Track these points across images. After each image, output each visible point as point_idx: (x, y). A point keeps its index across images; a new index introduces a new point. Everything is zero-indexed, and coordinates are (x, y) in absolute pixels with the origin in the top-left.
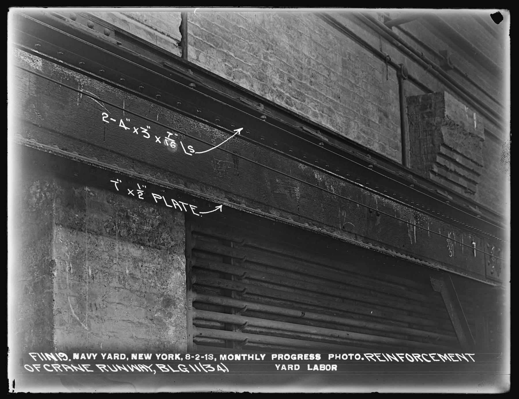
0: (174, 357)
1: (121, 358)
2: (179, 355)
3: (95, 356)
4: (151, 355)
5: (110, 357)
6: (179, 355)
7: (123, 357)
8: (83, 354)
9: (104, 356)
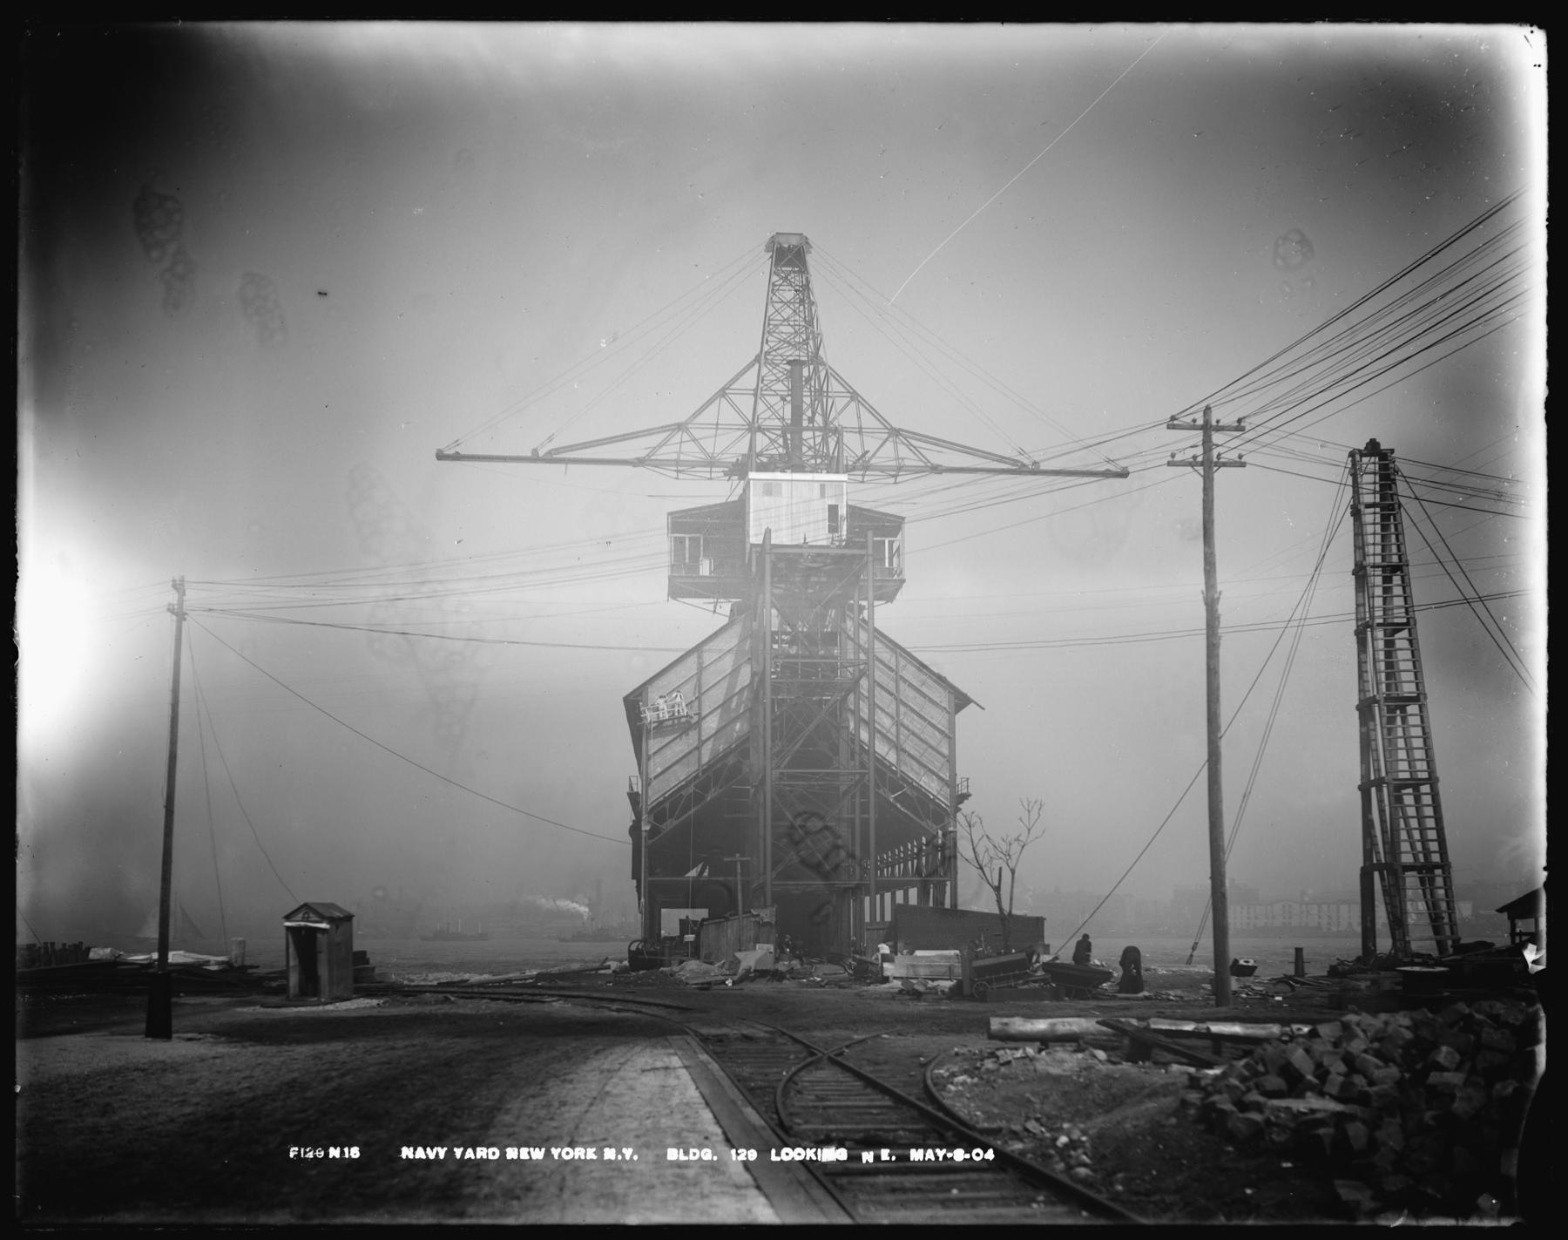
0: (585, 1154)
1: (491, 1157)
2: (594, 1150)
3: (442, 1152)
4: (543, 1150)
5: (469, 1154)
6: (594, 1150)
7: (494, 1154)
8: (420, 1149)
9: (458, 1152)
